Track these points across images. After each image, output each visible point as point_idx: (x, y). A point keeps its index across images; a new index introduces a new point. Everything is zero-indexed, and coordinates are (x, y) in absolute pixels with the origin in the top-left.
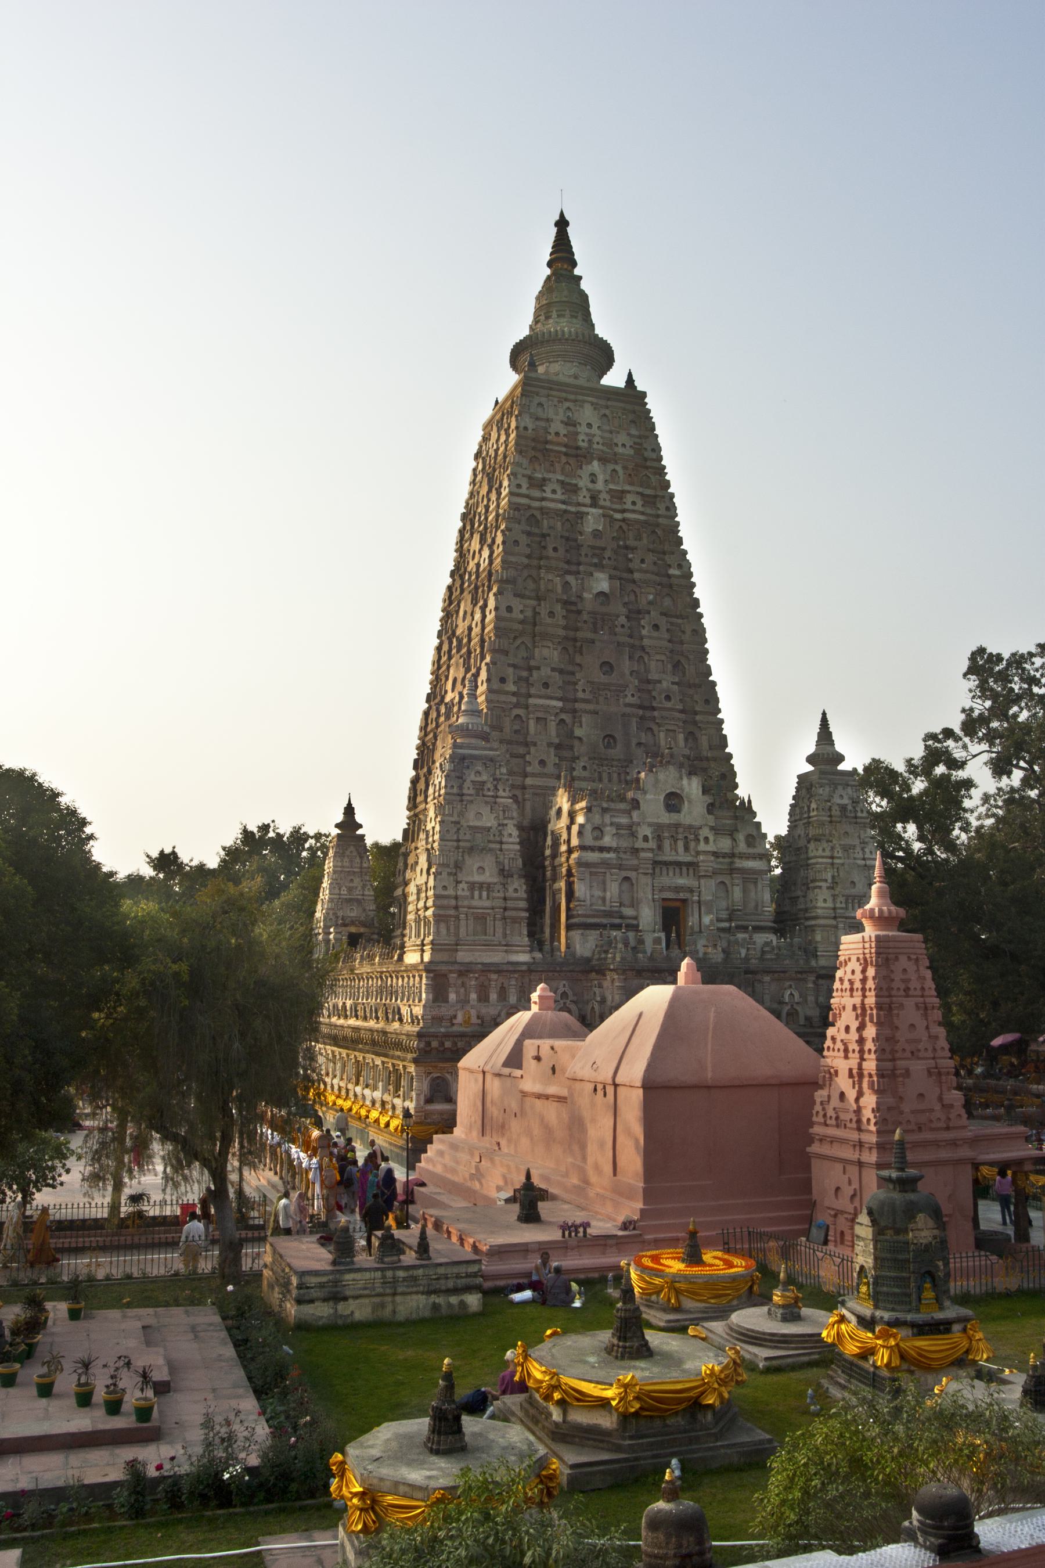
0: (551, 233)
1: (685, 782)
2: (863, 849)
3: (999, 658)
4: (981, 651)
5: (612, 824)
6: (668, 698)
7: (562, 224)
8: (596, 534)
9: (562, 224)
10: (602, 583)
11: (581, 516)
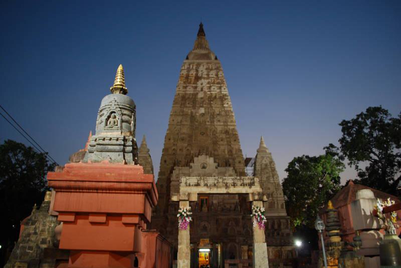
0: (198, 28)
1: (208, 159)
2: (273, 177)
3: (349, 122)
4: (344, 121)
5: (182, 173)
6: (222, 140)
7: (201, 26)
8: (202, 98)
9: (201, 26)
10: (202, 111)
11: (197, 94)
